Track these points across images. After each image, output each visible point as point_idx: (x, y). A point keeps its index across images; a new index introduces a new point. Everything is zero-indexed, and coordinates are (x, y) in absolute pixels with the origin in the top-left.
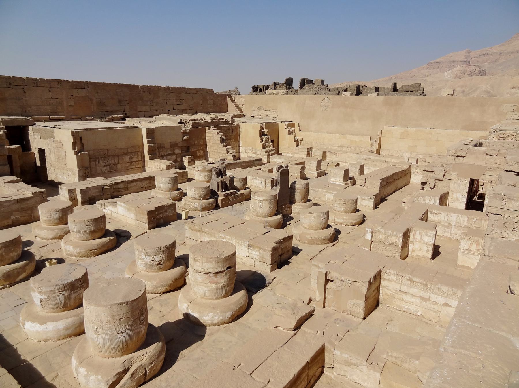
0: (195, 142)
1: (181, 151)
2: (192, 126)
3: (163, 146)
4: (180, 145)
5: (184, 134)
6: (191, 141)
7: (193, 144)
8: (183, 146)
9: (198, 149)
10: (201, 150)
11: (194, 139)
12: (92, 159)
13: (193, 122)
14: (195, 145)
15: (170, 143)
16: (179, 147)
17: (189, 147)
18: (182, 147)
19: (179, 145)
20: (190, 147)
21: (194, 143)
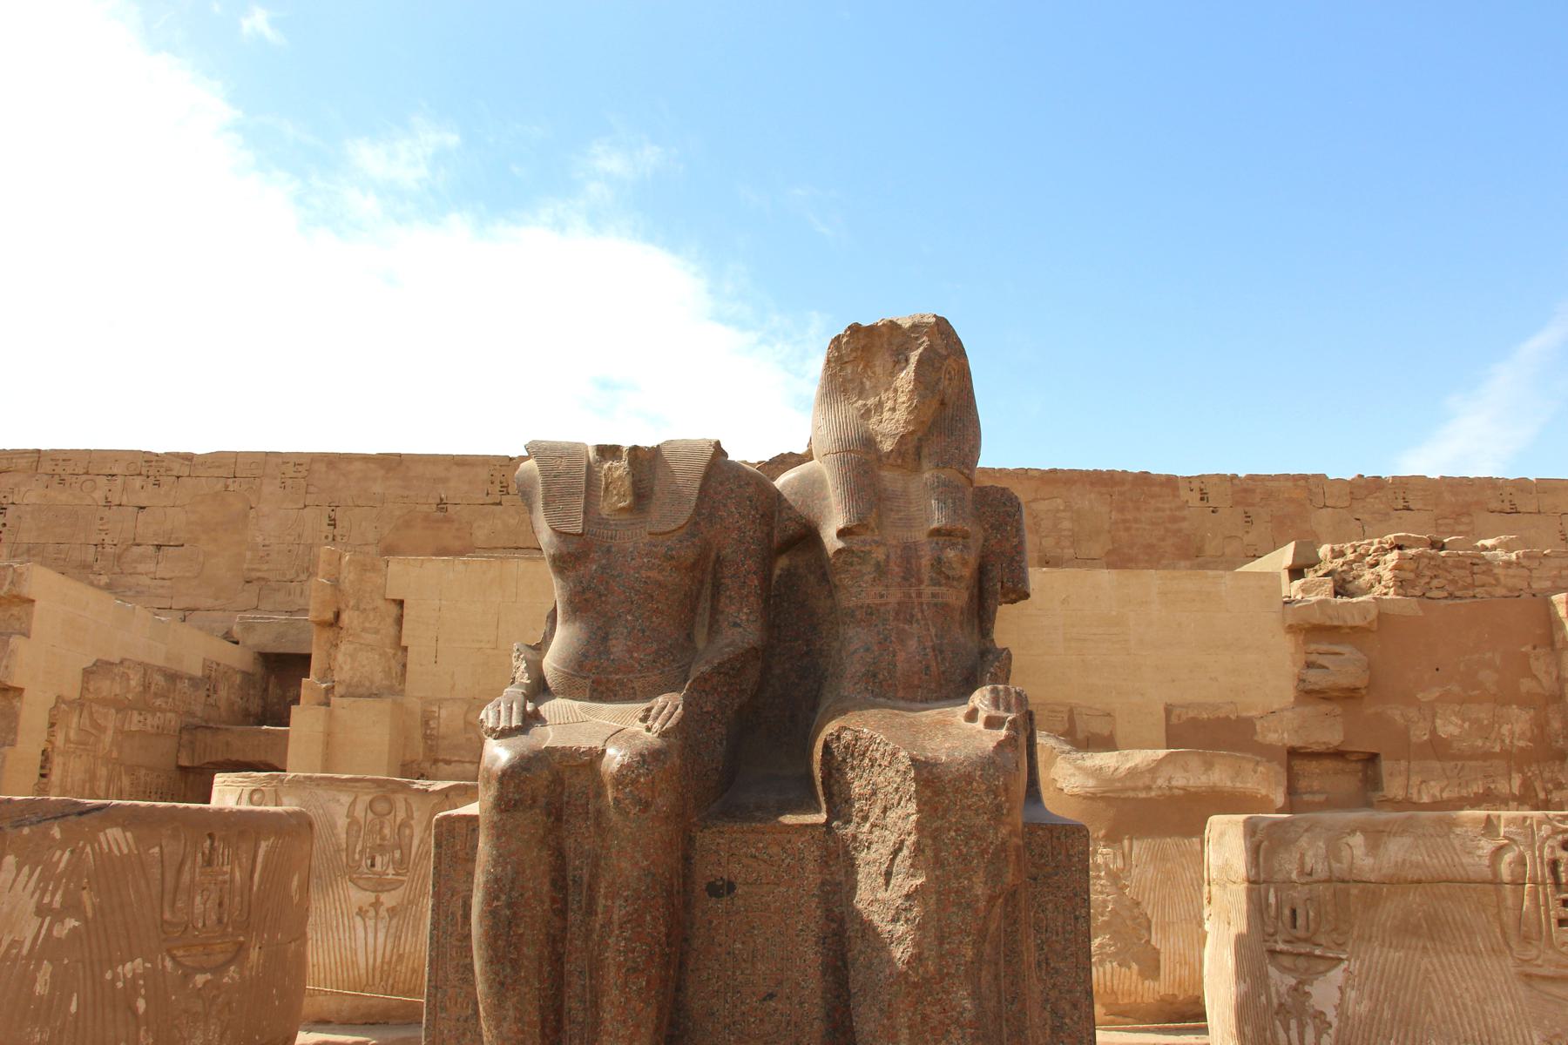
0: (1439, 722)
1: (1291, 791)
2: (1401, 584)
3: (1099, 727)
4: (1272, 738)
5: (1313, 647)
6: (1396, 713)
7: (1420, 734)
8: (1296, 742)
9: (1477, 788)
10: (1514, 798)
11: (1423, 697)
12: (448, 762)
13: (1410, 552)
14: (1438, 748)
15: (1168, 710)
16: (1265, 752)
17: (1372, 758)
18: (1293, 753)
19: (1259, 738)
20: (1385, 766)
21: (1433, 731)
